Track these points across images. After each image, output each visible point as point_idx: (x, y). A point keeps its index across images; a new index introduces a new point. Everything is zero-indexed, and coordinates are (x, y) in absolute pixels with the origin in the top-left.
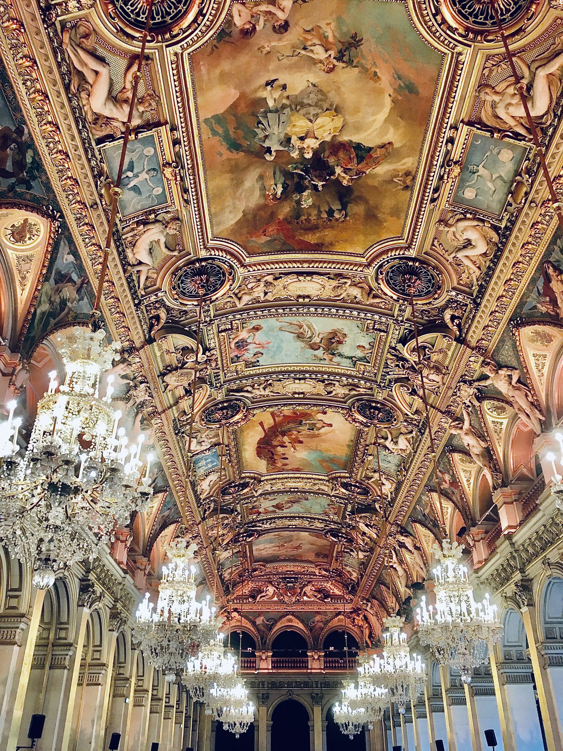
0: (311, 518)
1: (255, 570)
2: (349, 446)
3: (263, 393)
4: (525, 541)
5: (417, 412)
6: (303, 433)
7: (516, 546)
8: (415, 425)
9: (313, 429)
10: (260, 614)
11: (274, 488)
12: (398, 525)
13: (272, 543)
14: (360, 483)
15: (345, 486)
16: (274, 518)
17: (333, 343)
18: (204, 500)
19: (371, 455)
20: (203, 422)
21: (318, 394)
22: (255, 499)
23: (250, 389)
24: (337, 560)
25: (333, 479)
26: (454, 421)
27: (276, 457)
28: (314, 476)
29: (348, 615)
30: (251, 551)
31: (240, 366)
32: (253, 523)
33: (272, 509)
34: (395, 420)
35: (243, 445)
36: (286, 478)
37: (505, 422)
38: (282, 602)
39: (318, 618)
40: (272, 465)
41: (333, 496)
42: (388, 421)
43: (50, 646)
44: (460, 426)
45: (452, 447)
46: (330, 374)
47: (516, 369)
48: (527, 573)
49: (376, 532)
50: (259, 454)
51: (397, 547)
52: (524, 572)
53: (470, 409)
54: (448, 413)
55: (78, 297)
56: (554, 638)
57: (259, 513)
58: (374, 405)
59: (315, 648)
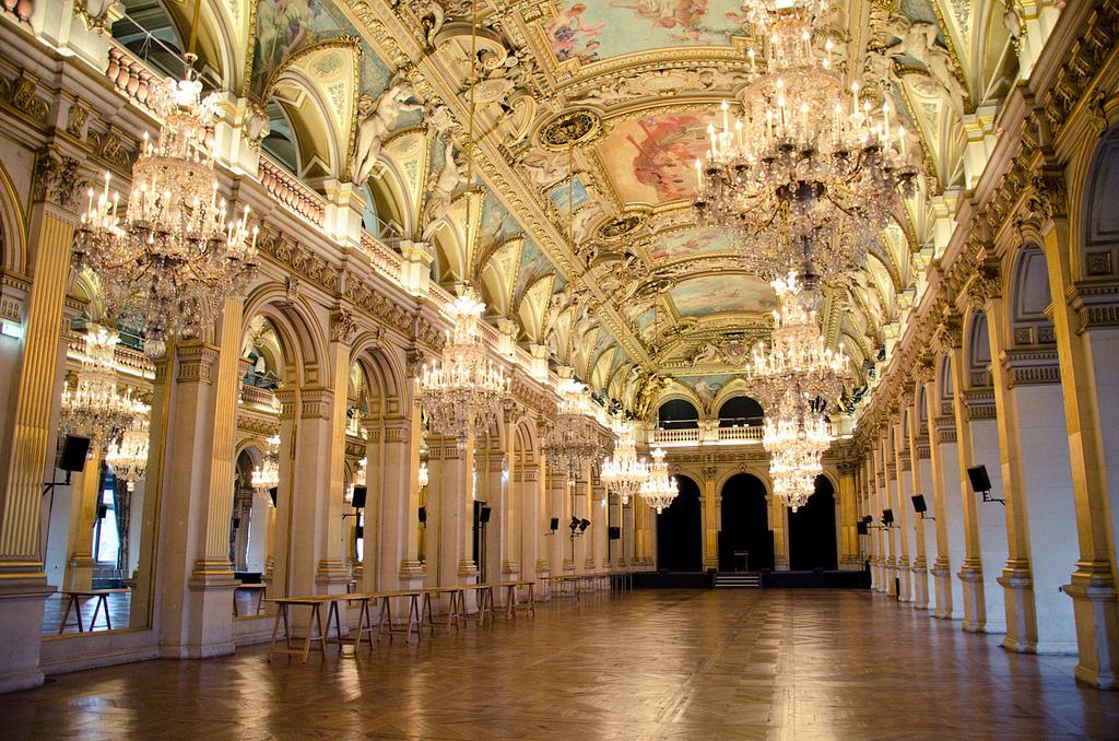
1: (685, 327)
3: (616, 96)
6: (691, 144)
10: (700, 379)
13: (697, 291)
16: (689, 261)
17: (691, 14)
22: (654, 238)
23: (596, 93)
30: (671, 304)
31: (571, 63)
33: (682, 249)
35: (613, 170)
43: (382, 419)
46: (701, 59)
47: (930, 23)
50: (640, 178)
51: (852, 287)
55: (311, 12)
56: (983, 385)
57: (667, 256)
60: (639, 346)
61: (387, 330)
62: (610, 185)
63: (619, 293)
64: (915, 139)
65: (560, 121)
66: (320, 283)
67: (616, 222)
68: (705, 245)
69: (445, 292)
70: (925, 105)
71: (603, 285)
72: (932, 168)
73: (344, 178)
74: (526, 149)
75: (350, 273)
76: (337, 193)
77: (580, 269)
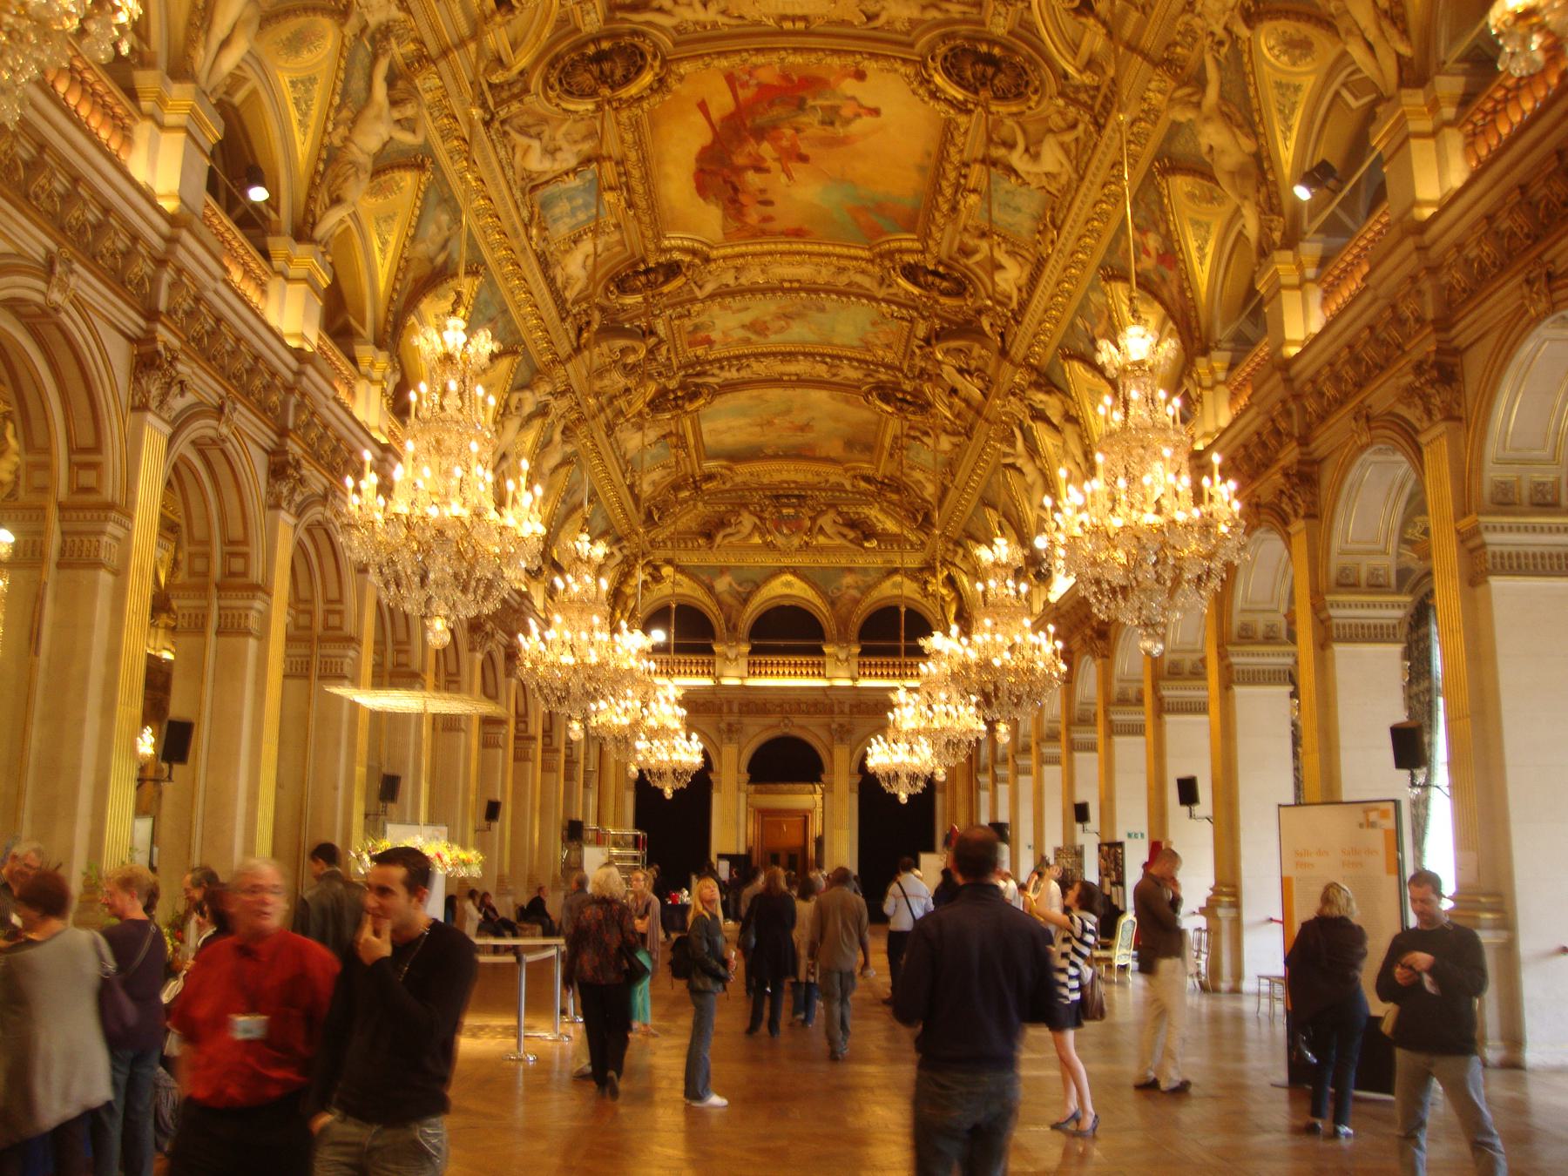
0: (832, 357)
2: (922, 169)
4: (1318, 372)
5: (1091, 64)
6: (809, 132)
7: (1297, 384)
8: (1084, 104)
9: (832, 123)
10: (722, 571)
11: (743, 280)
12: (1033, 368)
14: (947, 266)
15: (911, 273)
16: (747, 356)
18: (575, 303)
19: (974, 191)
20: (551, 94)
21: (843, 22)
22: (698, 306)
24: (891, 455)
25: (881, 256)
26: (1179, 87)
27: (743, 198)
28: (838, 250)
29: (913, 574)
30: (698, 434)
32: (697, 366)
33: (741, 333)
34: (1036, 91)
36: (771, 253)
37: (1308, 83)
38: (770, 547)
39: (848, 580)
40: (739, 220)
41: (884, 300)
42: (1019, 95)
44: (1195, 99)
45: (1170, 159)
48: (1313, 446)
49: (980, 384)
50: (702, 189)
52: (1307, 445)
53: (1224, 50)
54: (1167, 63)
57: (709, 342)
58: (984, 48)
59: (842, 639)
60: (629, 504)
61: (239, 406)
62: (650, 193)
63: (621, 403)
64: (1248, 145)
65: (591, 50)
66: (117, 280)
67: (642, 267)
68: (781, 330)
69: (338, 352)
70: (1279, 85)
71: (597, 385)
72: (1275, 201)
73: (180, 70)
74: (518, 97)
75: (180, 271)
76: (161, 101)
77: (564, 349)
